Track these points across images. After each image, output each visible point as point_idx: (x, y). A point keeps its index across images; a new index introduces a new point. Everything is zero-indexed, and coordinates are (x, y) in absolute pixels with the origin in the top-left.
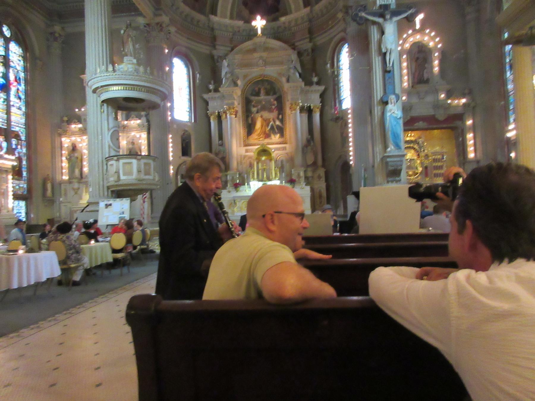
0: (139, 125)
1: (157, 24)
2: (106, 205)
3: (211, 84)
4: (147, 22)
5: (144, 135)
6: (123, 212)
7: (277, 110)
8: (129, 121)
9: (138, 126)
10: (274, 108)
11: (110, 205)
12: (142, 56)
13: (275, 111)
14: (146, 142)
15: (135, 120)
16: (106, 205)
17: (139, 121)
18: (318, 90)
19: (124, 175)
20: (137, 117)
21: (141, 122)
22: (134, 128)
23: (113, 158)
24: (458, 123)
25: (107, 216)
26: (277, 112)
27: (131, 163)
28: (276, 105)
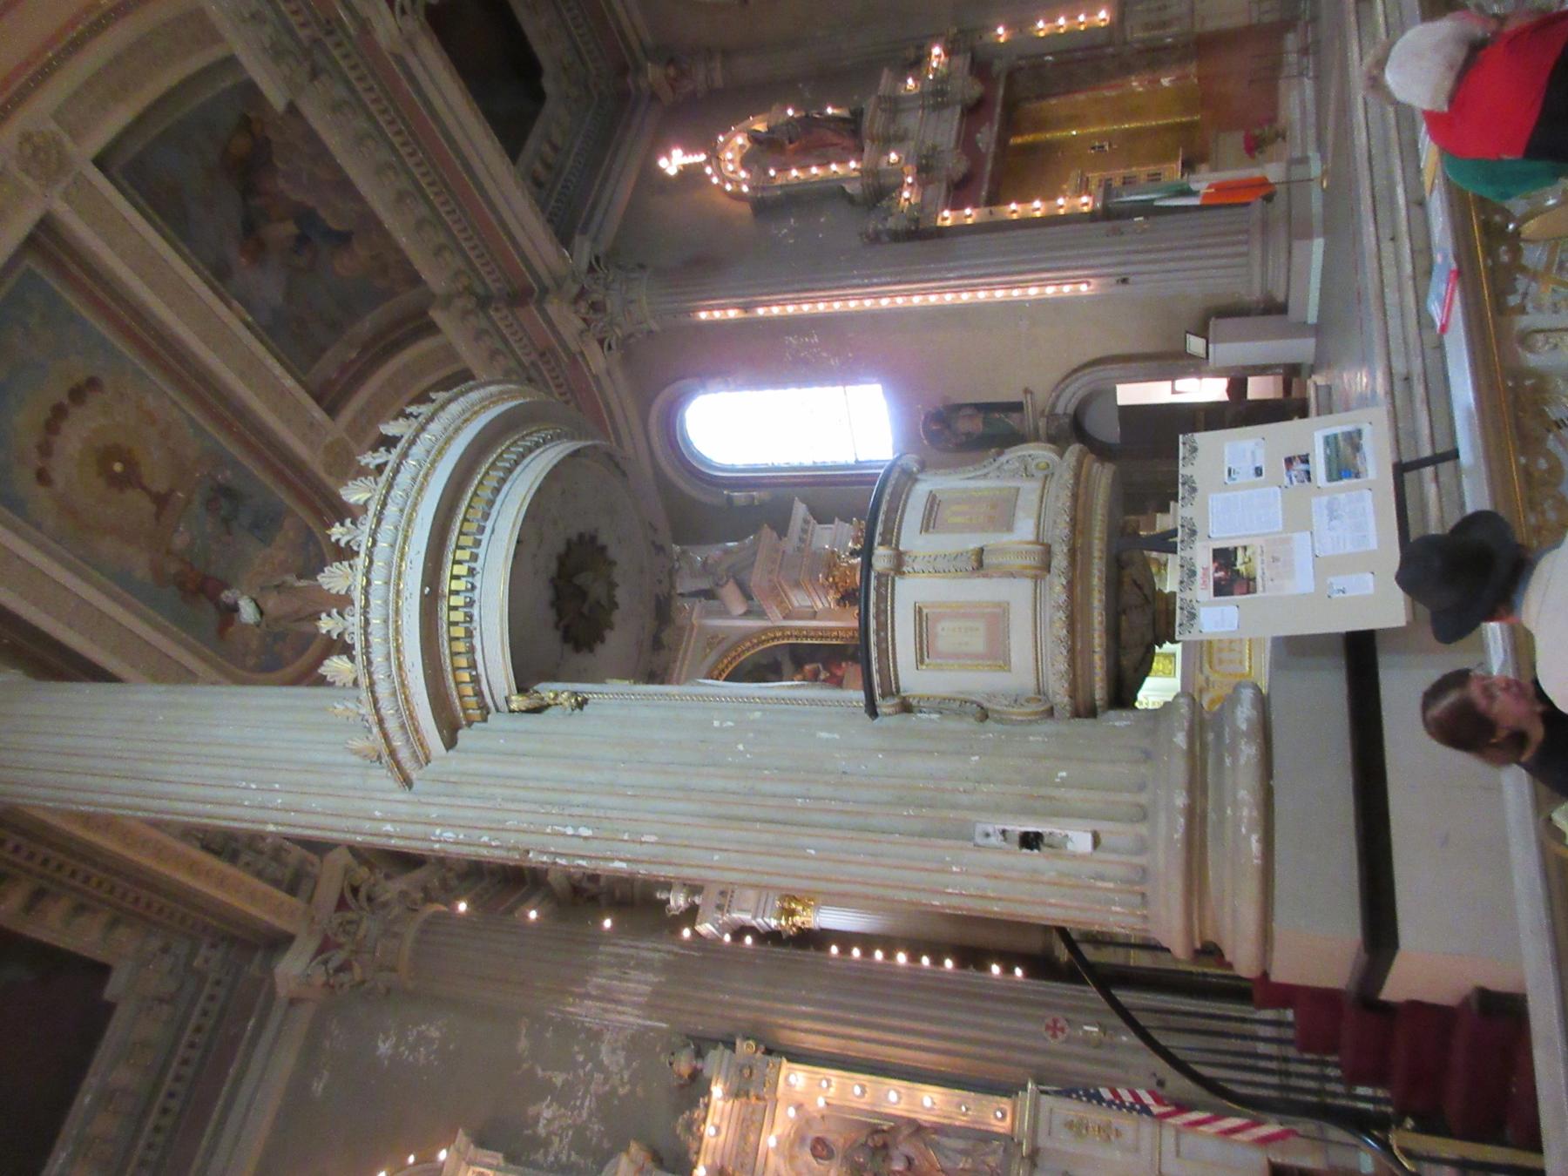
0: (736, 1093)
1: (342, 905)
2: (1221, 589)
3: (668, 901)
4: (313, 945)
5: (796, 1077)
6: (1289, 461)
7: (839, 666)
8: (698, 1153)
9: (737, 1096)
10: (828, 675)
11: (1224, 557)
12: (435, 1033)
13: (839, 673)
14: (835, 1075)
15: (704, 1120)
16: (1221, 589)
17: (717, 1090)
18: (806, 522)
19: (1009, 528)
20: (693, 1104)
21: (725, 1084)
22: (744, 1138)
23: (879, 576)
24: (998, 66)
25: (1324, 566)
26: (844, 665)
27: (933, 502)
28: (820, 666)
